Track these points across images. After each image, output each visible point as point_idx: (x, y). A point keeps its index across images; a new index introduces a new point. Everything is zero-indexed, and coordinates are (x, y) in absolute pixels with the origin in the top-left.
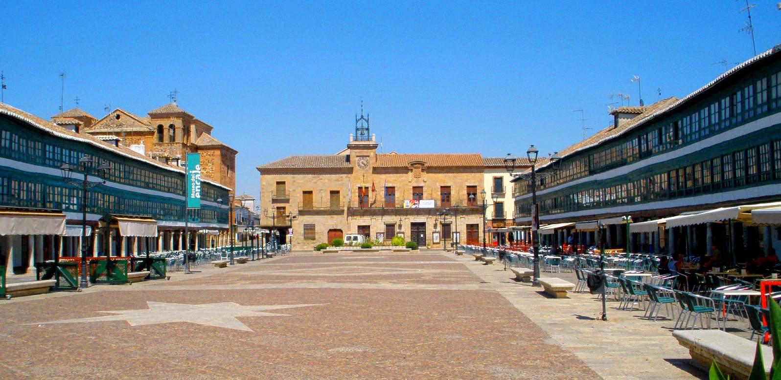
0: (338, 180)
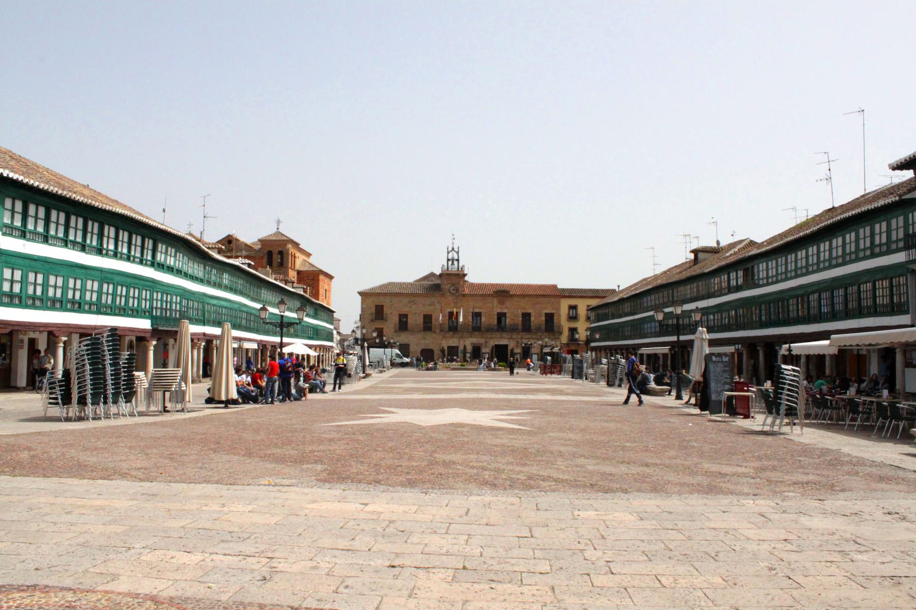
0: (430, 305)
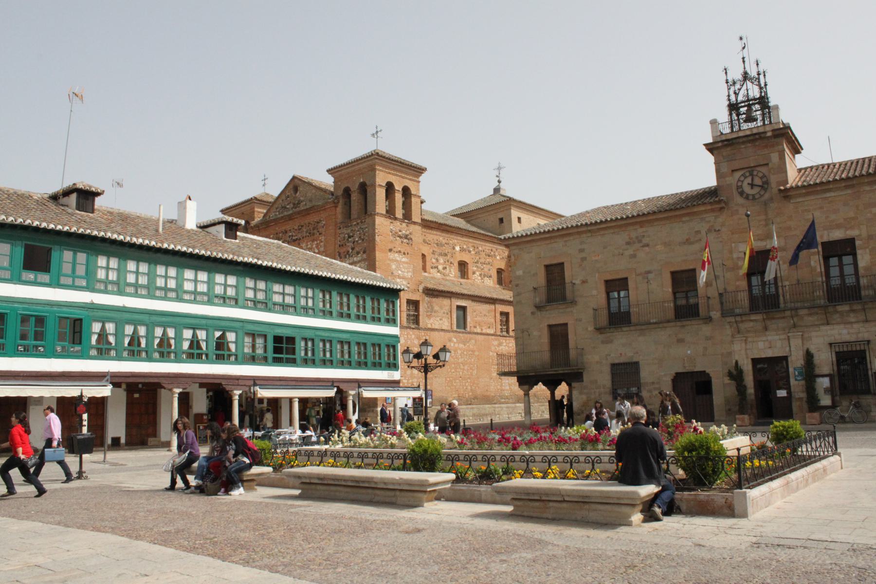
0: (688, 242)
